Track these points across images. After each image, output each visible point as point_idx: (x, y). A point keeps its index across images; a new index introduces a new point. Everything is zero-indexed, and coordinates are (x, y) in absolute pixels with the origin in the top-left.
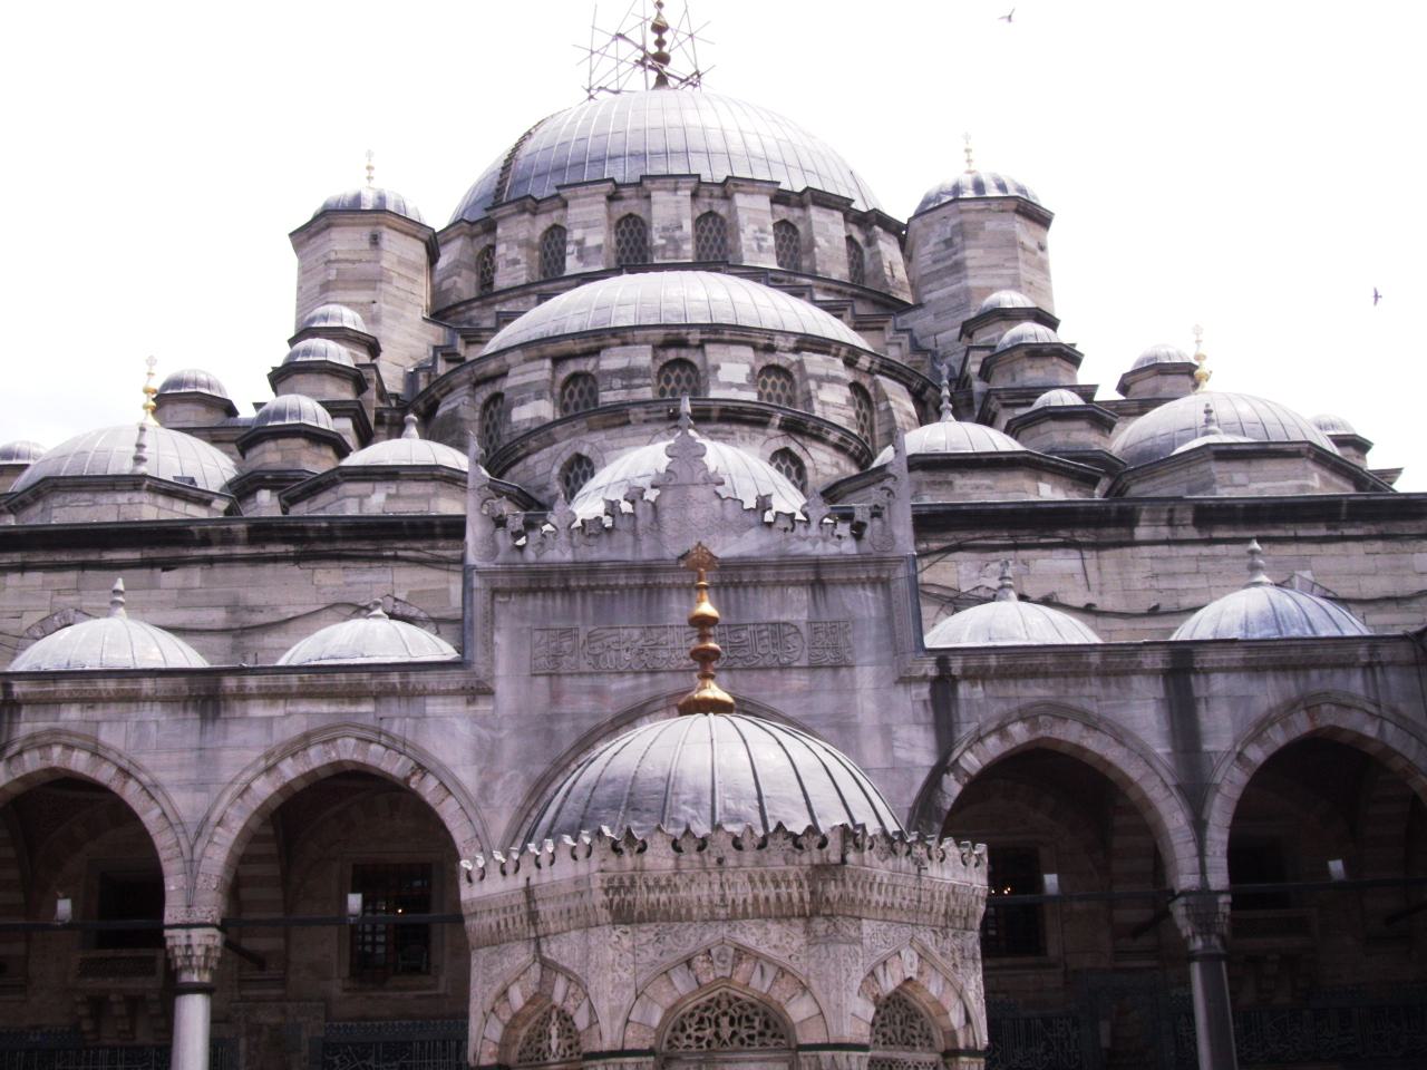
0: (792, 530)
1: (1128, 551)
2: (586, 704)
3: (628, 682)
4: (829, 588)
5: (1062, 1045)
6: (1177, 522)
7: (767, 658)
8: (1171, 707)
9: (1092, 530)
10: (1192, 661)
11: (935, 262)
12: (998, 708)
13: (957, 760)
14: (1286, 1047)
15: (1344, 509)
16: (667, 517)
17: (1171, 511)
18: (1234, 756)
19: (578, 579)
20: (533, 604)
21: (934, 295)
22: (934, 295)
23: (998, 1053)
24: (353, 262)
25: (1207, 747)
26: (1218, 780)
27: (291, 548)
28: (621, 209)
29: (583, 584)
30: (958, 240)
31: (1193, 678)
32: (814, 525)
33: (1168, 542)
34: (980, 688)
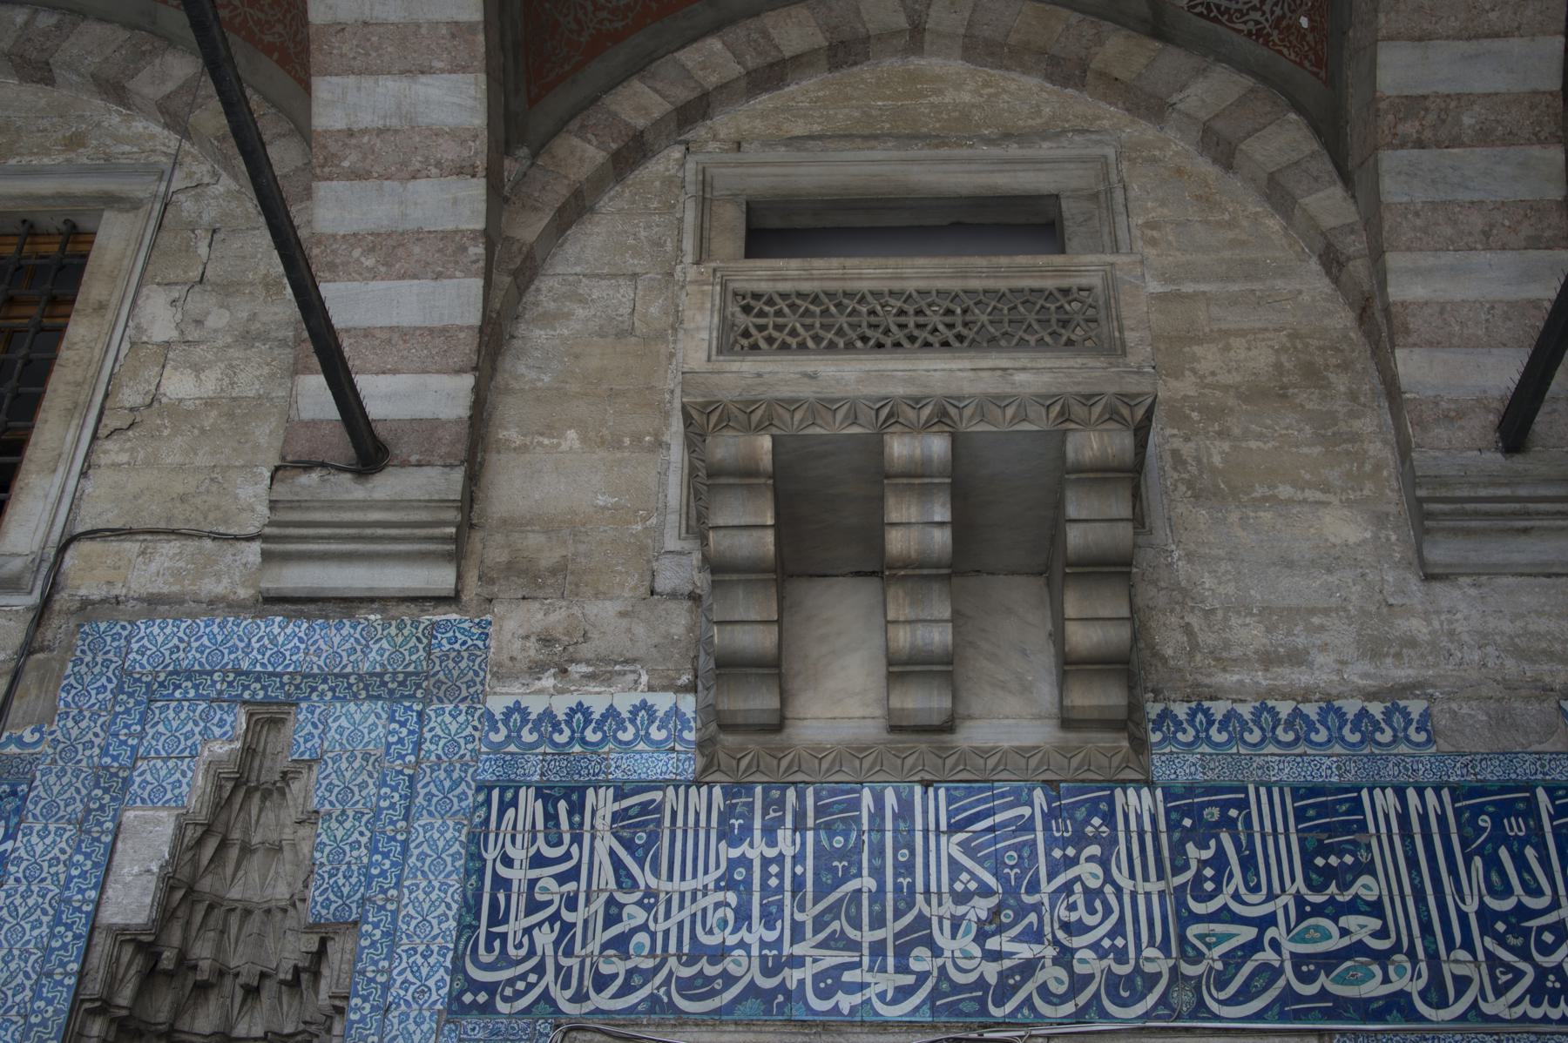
14: (1025, 951)
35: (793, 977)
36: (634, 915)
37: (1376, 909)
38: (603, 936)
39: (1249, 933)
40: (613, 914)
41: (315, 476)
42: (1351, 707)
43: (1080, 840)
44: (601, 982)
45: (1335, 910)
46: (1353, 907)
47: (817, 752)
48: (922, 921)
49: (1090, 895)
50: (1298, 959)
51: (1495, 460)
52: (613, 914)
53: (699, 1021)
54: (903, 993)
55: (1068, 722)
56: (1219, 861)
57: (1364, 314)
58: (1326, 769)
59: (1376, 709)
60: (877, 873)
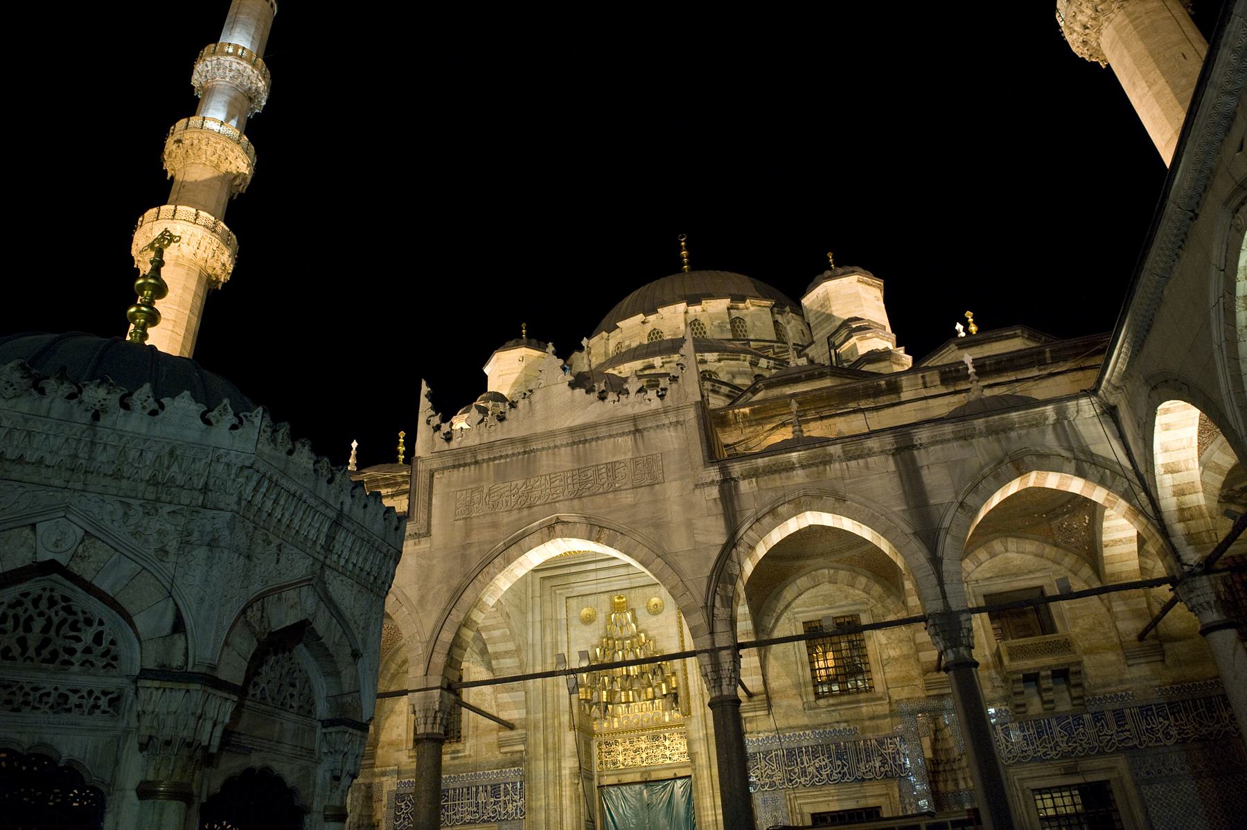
0: (619, 401)
1: (897, 408)
2: (486, 535)
3: (515, 515)
4: (646, 433)
5: (894, 758)
6: (929, 385)
7: (606, 485)
8: (900, 476)
9: (871, 400)
10: (912, 439)
11: (817, 319)
12: (768, 496)
13: (742, 538)
14: (1074, 745)
15: (1048, 355)
16: (538, 407)
17: (923, 377)
18: (958, 504)
19: (482, 455)
20: (456, 475)
21: (819, 335)
22: (819, 335)
23: (845, 769)
24: (510, 374)
25: (932, 502)
26: (946, 524)
27: (389, 490)
28: (648, 328)
29: (486, 457)
30: (827, 303)
31: (915, 452)
32: (632, 394)
33: (925, 398)
34: (755, 484)
35: (1039, 754)
36: (1010, 747)
37: (1129, 731)
38: (1006, 751)
39: (1109, 737)
40: (1007, 747)
41: (930, 674)
42: (1119, 694)
43: (1079, 725)
44: (1009, 758)
45: (1123, 732)
46: (1126, 730)
47: (1032, 716)
48: (1057, 742)
49: (1083, 734)
50: (1118, 741)
51: (1137, 643)
52: (1007, 747)
53: (1026, 763)
54: (1057, 755)
55: (1074, 705)
56: (1102, 725)
57: (1109, 610)
58: (1117, 706)
59: (1124, 694)
60: (1047, 735)
